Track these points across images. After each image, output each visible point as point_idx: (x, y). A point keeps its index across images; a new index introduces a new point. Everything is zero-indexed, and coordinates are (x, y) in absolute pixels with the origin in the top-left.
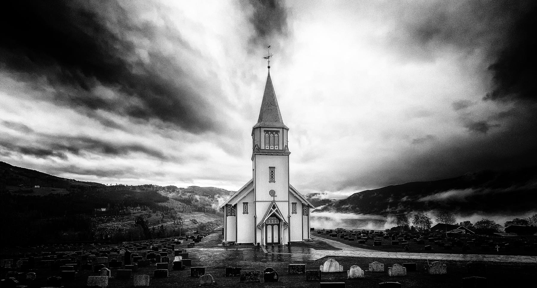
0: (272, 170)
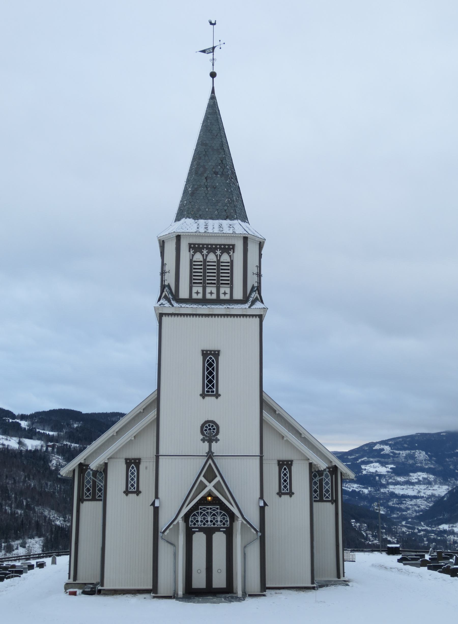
0: (211, 360)
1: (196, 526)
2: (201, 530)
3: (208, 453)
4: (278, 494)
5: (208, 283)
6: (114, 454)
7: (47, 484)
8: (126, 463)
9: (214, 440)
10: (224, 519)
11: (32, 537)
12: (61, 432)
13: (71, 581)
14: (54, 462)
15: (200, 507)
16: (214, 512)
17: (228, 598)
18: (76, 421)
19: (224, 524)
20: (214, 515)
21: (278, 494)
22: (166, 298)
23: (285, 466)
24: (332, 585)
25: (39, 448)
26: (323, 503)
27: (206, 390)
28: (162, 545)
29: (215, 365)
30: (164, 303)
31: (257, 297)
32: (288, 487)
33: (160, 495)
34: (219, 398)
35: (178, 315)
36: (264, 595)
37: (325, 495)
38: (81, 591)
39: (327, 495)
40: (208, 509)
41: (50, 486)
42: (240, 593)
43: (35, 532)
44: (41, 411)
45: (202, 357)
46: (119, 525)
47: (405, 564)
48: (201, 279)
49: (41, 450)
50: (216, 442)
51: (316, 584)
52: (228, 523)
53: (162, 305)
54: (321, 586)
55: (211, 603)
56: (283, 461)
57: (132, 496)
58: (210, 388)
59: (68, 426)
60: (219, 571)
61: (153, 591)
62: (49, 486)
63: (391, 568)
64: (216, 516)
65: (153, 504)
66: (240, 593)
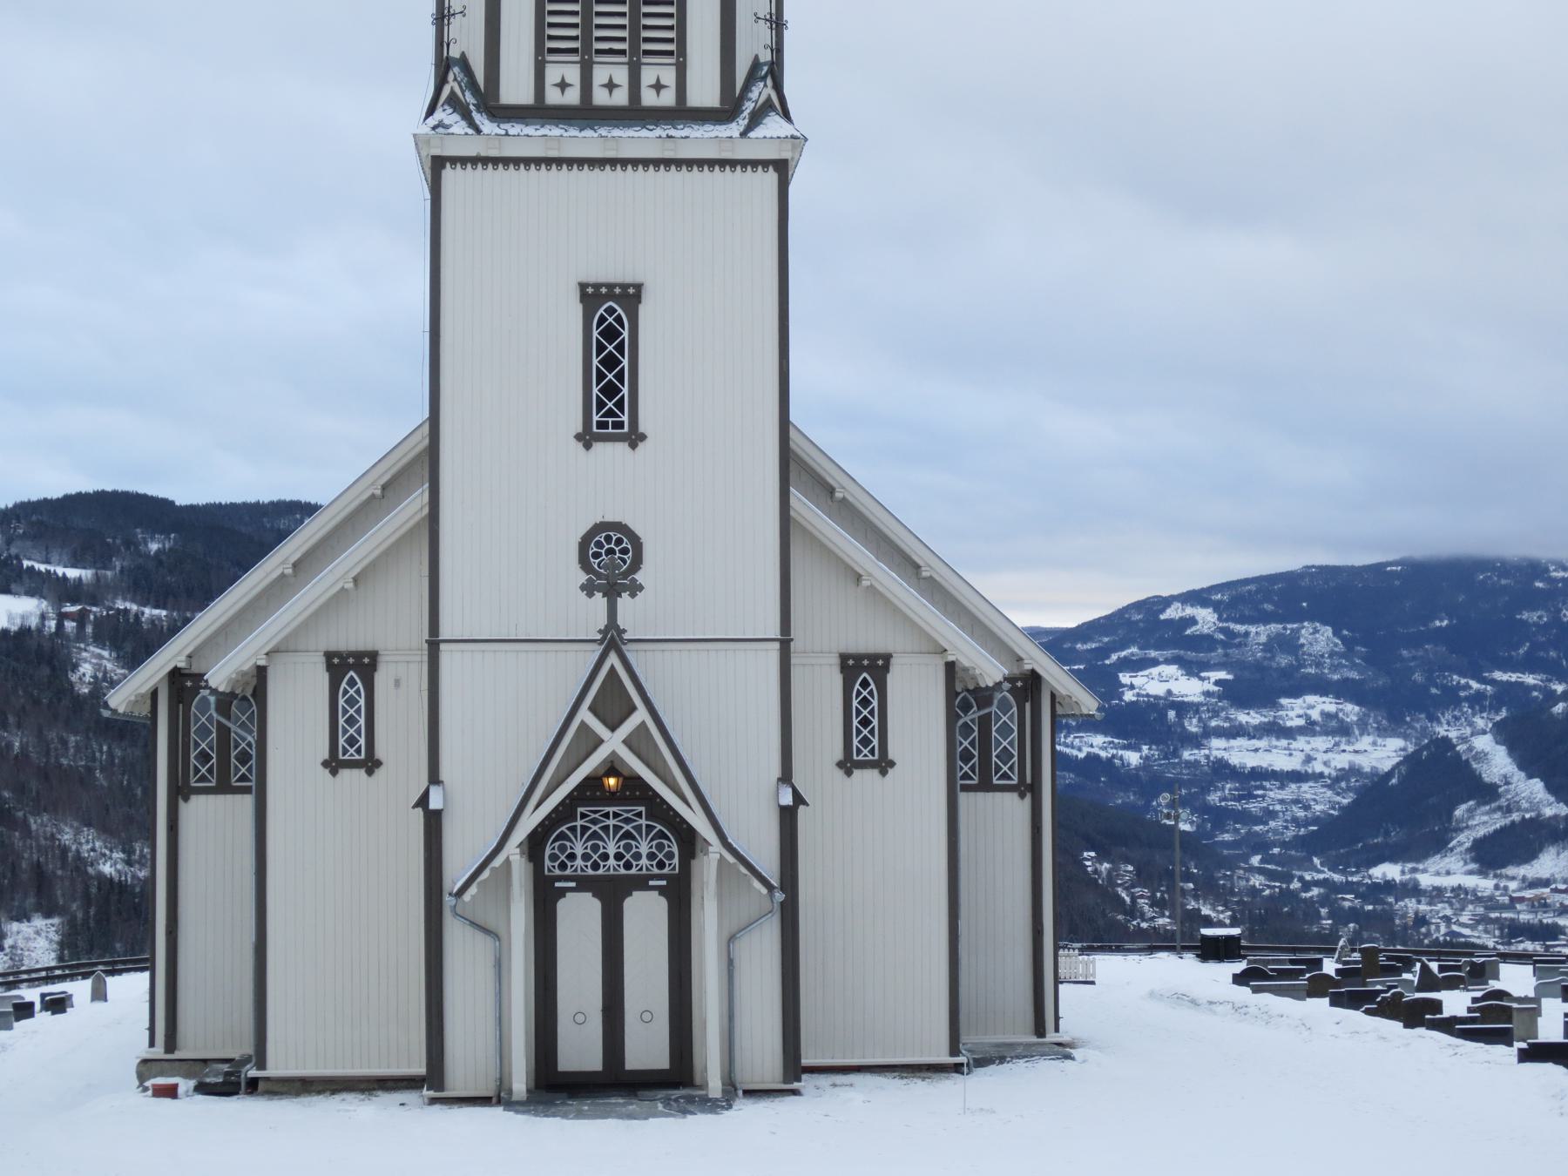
0: (610, 316)
1: (568, 872)
2: (584, 884)
3: (604, 632)
4: (840, 765)
5: (599, 52)
6: (286, 638)
7: (64, 743)
8: (330, 667)
9: (624, 588)
10: (660, 847)
11: (23, 916)
12: (105, 568)
13: (159, 1052)
14: (86, 669)
15: (580, 810)
16: (627, 827)
17: (676, 1100)
18: (154, 532)
19: (661, 865)
20: (628, 835)
21: (840, 765)
22: (455, 103)
23: (864, 672)
24: (1018, 1057)
25: (33, 622)
26: (990, 795)
27: (596, 418)
28: (456, 935)
29: (626, 334)
30: (446, 122)
31: (769, 99)
32: (875, 742)
33: (445, 773)
34: (641, 445)
35: (496, 161)
36: (795, 1092)
37: (998, 769)
38: (192, 1083)
39: (1005, 768)
40: (607, 815)
41: (77, 747)
42: (715, 1087)
43: (31, 901)
44: (34, 498)
45: (580, 307)
46: (312, 871)
47: (1256, 990)
48: (576, 38)
49: (40, 630)
50: (633, 595)
51: (963, 1056)
52: (676, 861)
53: (440, 130)
54: (981, 1063)
55: (621, 1116)
56: (859, 658)
57: (352, 778)
58: (610, 413)
59: (128, 548)
60: (646, 1017)
61: (431, 1081)
62: (71, 749)
63: (1211, 1003)
64: (634, 838)
65: (423, 801)
66: (715, 1087)
